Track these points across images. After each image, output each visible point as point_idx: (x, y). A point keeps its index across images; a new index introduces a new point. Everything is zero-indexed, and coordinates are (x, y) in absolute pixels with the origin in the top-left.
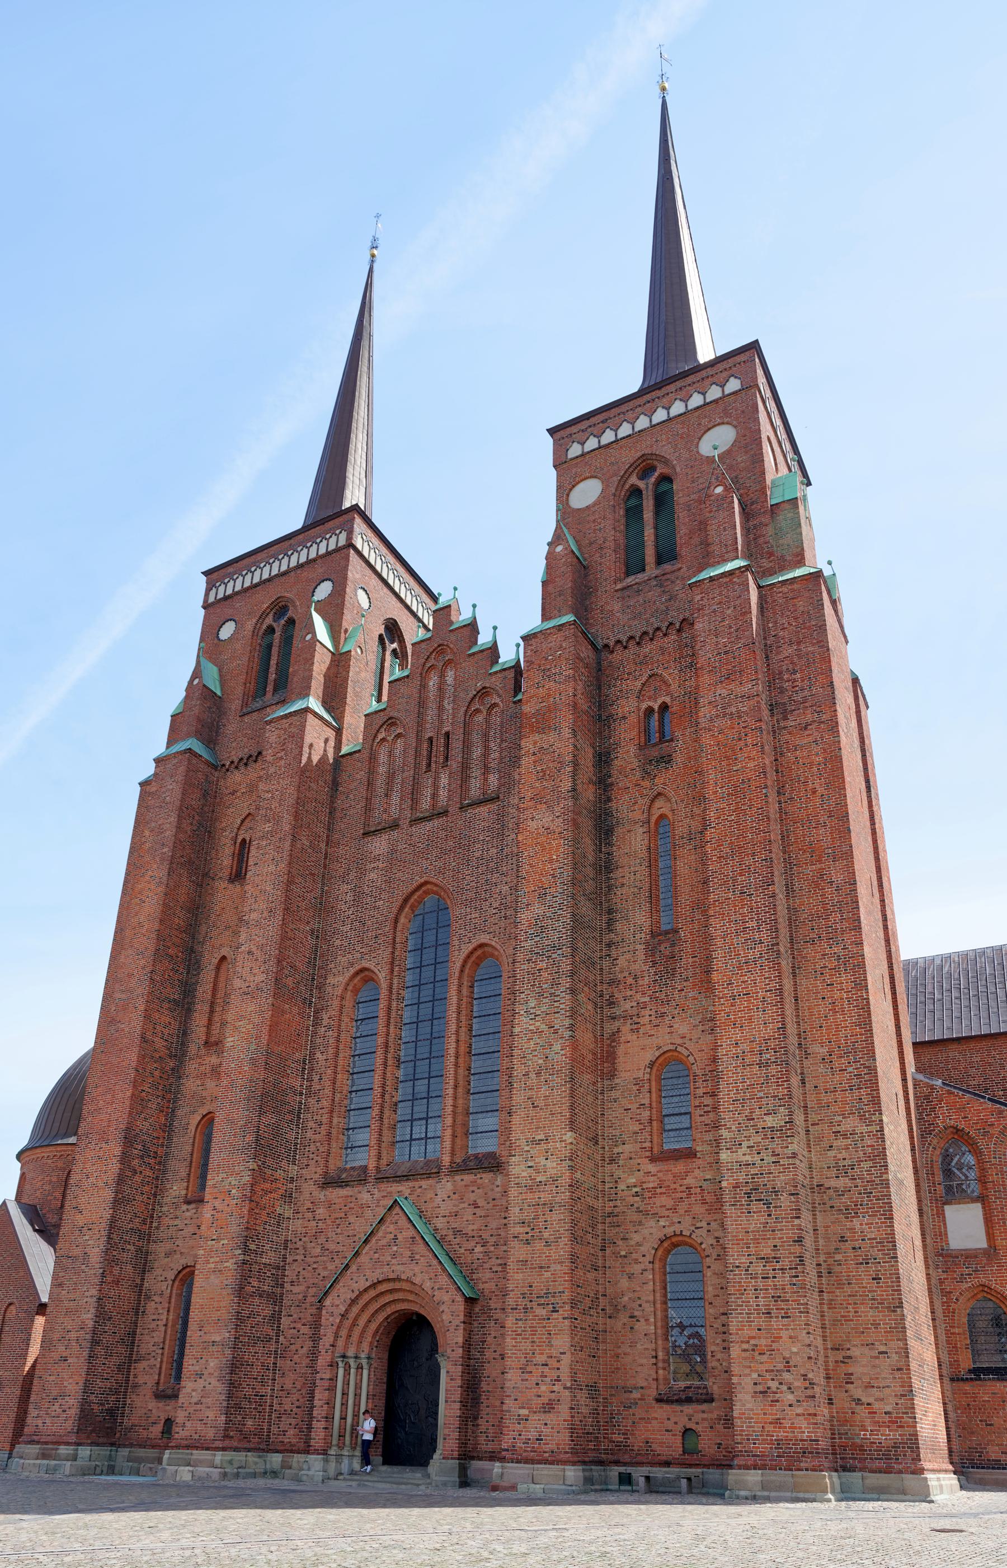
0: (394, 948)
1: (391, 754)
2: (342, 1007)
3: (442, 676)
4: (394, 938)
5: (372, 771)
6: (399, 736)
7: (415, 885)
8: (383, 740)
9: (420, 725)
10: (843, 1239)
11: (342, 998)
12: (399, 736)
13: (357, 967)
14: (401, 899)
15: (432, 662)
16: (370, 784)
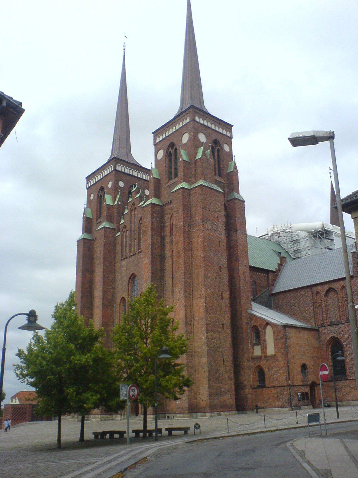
0: (128, 291)
1: (126, 236)
2: (120, 307)
3: (135, 212)
4: (128, 289)
5: (122, 241)
6: (127, 230)
7: (131, 274)
8: (124, 232)
9: (131, 227)
10: (199, 363)
11: (120, 305)
12: (127, 230)
13: (122, 297)
14: (129, 278)
15: (132, 208)
16: (122, 245)
